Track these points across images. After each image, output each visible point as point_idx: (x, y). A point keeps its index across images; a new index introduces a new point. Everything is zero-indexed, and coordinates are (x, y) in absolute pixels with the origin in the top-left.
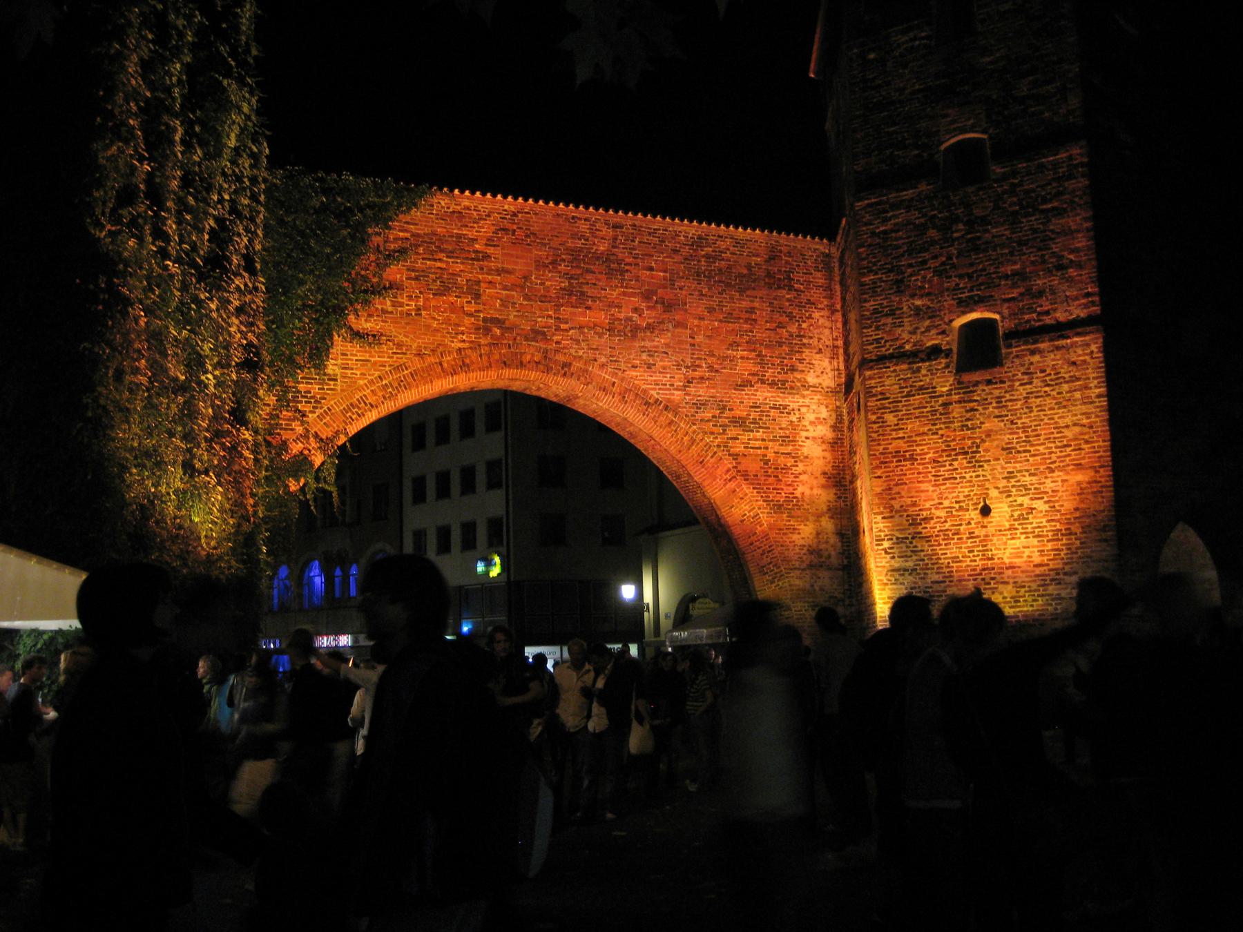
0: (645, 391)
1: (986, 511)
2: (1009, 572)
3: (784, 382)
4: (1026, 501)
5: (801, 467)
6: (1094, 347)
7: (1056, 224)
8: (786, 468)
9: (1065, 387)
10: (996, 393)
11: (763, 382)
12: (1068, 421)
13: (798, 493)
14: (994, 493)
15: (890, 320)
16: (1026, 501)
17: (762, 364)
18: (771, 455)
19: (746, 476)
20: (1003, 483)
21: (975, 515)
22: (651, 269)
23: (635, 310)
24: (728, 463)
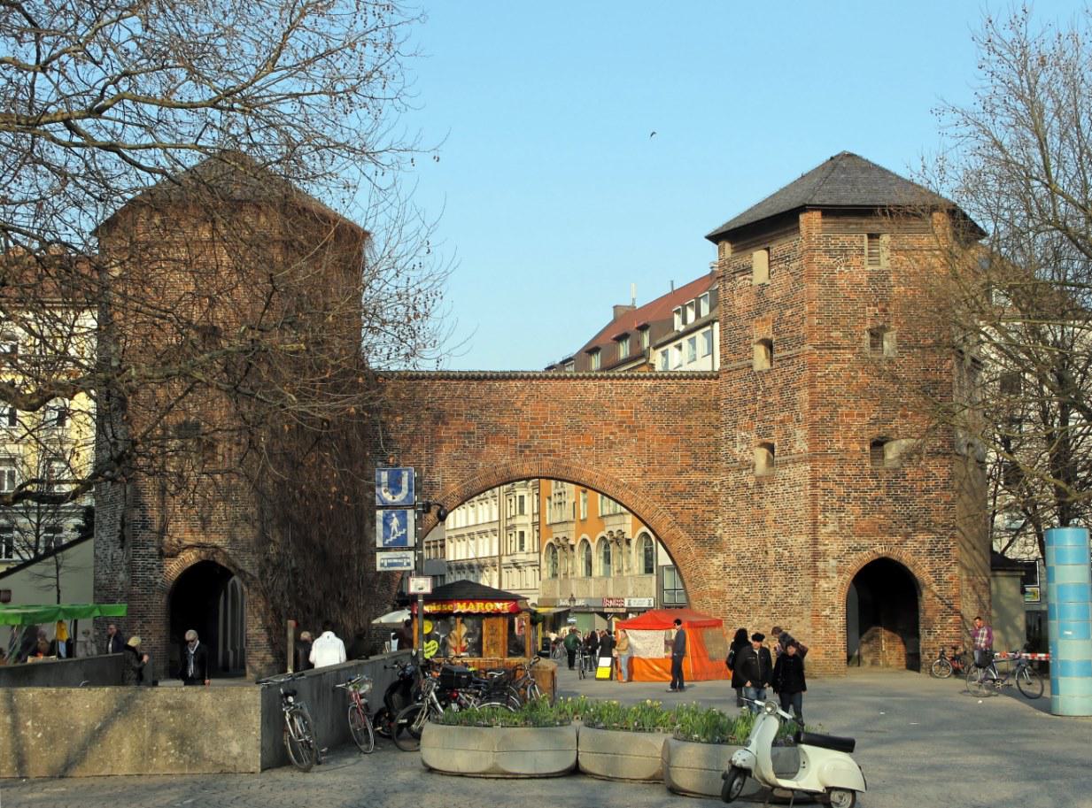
0: (617, 480)
1: (766, 552)
2: (773, 589)
3: (710, 468)
8: (710, 520)
9: (797, 489)
10: (771, 489)
11: (696, 469)
13: (717, 534)
14: (769, 545)
15: (731, 443)
16: (780, 550)
18: (699, 512)
19: (681, 525)
20: (772, 540)
22: (623, 408)
23: (612, 433)
24: (670, 518)
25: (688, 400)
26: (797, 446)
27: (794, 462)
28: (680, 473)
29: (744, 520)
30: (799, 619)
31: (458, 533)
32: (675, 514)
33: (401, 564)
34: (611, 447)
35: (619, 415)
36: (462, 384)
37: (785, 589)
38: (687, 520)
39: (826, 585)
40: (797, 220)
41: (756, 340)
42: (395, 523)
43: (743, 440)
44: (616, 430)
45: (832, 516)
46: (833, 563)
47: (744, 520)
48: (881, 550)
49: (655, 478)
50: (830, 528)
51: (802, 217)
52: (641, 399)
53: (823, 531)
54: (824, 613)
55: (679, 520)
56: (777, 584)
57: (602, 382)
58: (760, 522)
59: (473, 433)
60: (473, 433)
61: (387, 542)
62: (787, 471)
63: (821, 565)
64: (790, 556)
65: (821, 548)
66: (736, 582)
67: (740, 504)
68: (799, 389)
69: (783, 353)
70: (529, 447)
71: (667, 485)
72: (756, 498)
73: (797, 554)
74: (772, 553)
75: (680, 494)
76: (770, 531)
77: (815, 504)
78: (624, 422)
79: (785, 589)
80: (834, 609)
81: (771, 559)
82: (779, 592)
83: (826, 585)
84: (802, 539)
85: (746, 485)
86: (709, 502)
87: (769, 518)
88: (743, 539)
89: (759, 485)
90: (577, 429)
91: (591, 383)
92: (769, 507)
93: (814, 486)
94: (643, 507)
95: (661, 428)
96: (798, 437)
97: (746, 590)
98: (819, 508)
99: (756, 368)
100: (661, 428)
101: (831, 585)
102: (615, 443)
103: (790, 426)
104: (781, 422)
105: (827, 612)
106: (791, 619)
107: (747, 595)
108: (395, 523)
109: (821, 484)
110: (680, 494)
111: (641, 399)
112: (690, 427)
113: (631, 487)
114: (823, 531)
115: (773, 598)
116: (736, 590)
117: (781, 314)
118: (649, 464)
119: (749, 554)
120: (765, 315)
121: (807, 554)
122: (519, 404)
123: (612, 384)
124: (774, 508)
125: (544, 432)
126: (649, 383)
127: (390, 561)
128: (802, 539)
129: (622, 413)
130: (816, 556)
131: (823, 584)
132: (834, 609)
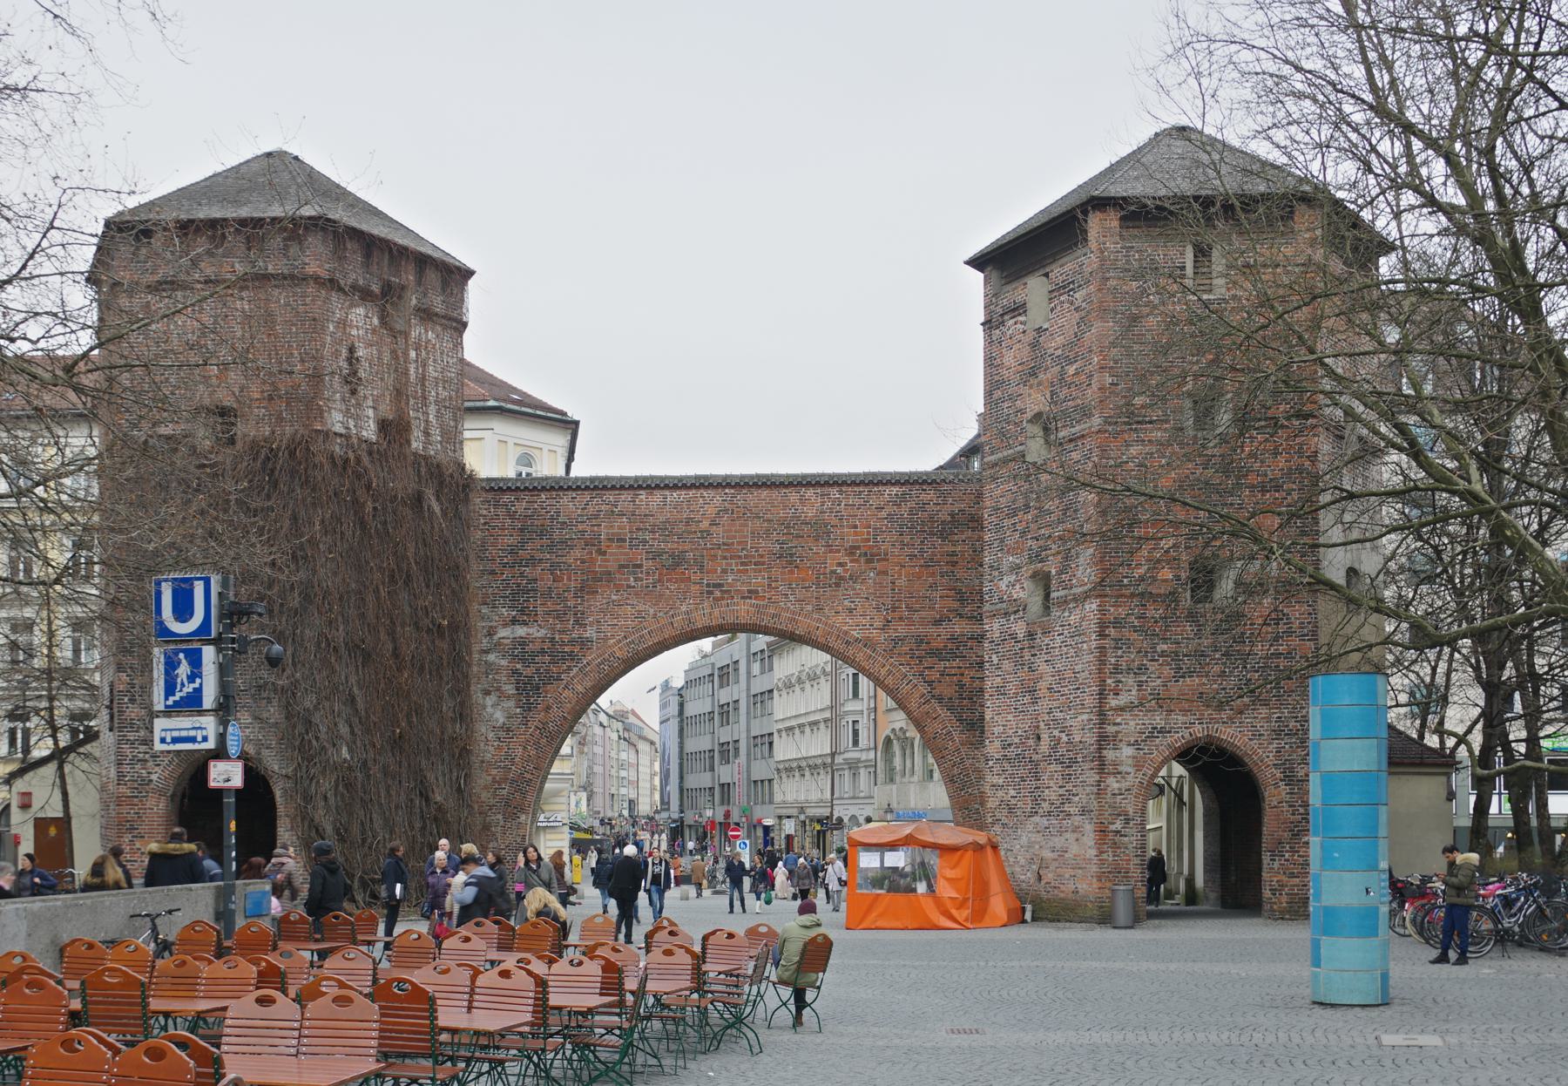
0: (846, 633)
1: (1039, 738)
6: (1094, 606)
11: (961, 616)
16: (1056, 733)
17: (961, 600)
19: (940, 699)
21: (1031, 742)
23: (840, 565)
25: (952, 515)
28: (937, 622)
29: (1011, 688)
31: (812, 718)
32: (930, 683)
33: (193, 740)
34: (837, 585)
35: (851, 540)
36: (626, 496)
37: (1062, 791)
38: (948, 691)
39: (1116, 785)
41: (1029, 415)
42: (183, 670)
44: (847, 559)
45: (1130, 680)
46: (1128, 751)
47: (1011, 688)
48: (1199, 731)
49: (901, 630)
50: (1123, 700)
52: (884, 514)
53: (1114, 703)
54: (1113, 827)
55: (936, 692)
57: (826, 490)
58: (1032, 691)
59: (640, 566)
60: (640, 566)
61: (170, 702)
63: (1110, 755)
65: (1111, 729)
70: (720, 585)
71: (920, 640)
74: (1045, 736)
75: (937, 654)
76: (1044, 705)
77: (1102, 662)
78: (858, 548)
79: (1062, 791)
80: (1127, 821)
81: (1044, 747)
83: (1116, 785)
85: (1013, 636)
87: (1043, 685)
88: (1010, 717)
89: (1031, 635)
90: (787, 558)
91: (810, 492)
92: (1043, 668)
93: (1102, 635)
94: (883, 672)
95: (912, 557)
97: (1013, 793)
98: (1108, 668)
100: (912, 557)
101: (1124, 785)
102: (842, 578)
105: (1118, 825)
107: (1013, 801)
108: (183, 670)
109: (1112, 631)
110: (937, 654)
111: (884, 514)
112: (954, 554)
113: (867, 643)
116: (1000, 793)
117: (1062, 373)
118: (894, 609)
119: (1017, 740)
121: (1090, 738)
122: (705, 524)
123: (841, 492)
124: (1049, 669)
125: (743, 564)
126: (895, 490)
127: (176, 734)
129: (856, 534)
130: (1103, 740)
131: (1113, 783)
132: (1127, 821)
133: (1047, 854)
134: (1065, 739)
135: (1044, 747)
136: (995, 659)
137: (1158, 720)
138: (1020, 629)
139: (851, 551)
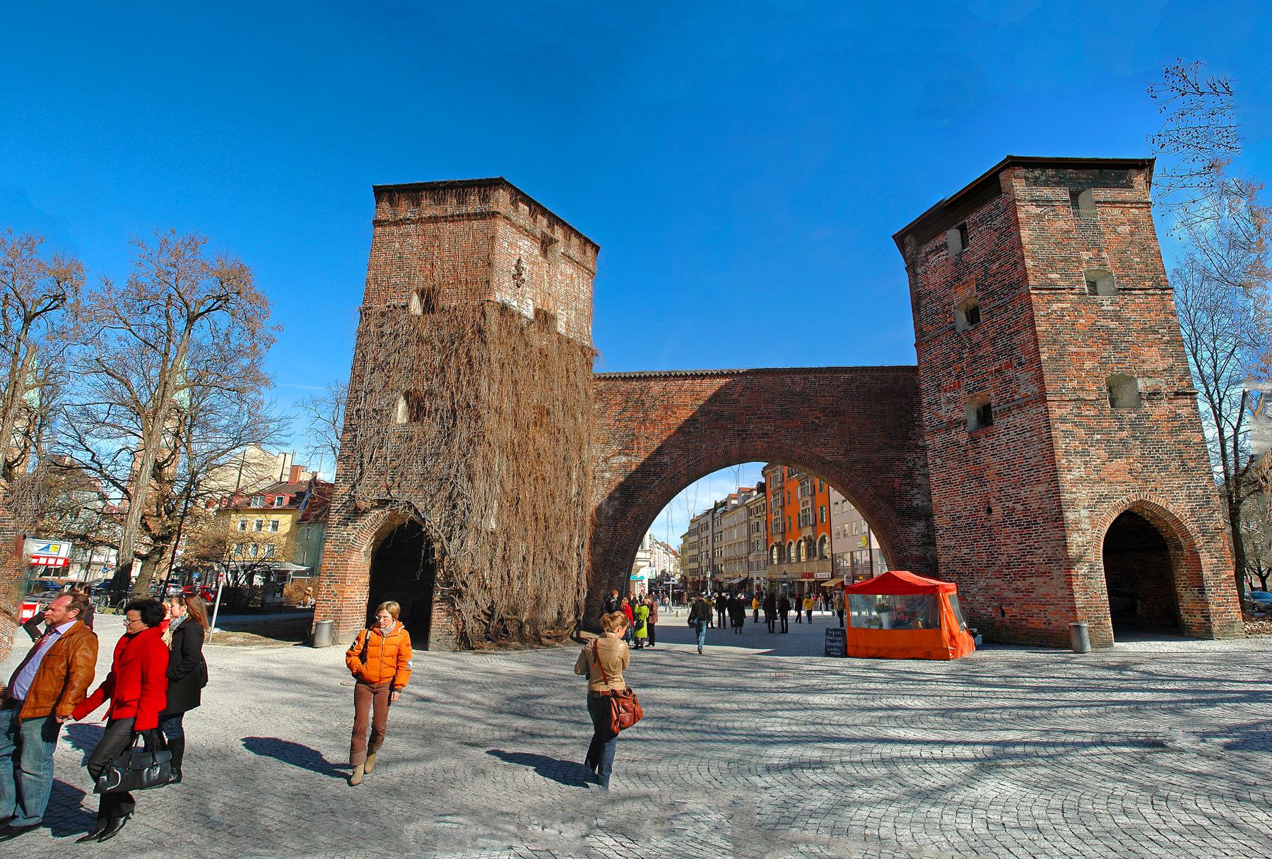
1: (990, 511)
4: (1010, 504)
5: (915, 491)
7: (1016, 339)
9: (1028, 434)
12: (1031, 454)
16: (1010, 504)
18: (896, 485)
21: (983, 514)
26: (1022, 391)
27: (1019, 407)
28: (877, 451)
30: (1048, 580)
32: (875, 487)
37: (1020, 547)
40: (998, 179)
43: (949, 401)
46: (1084, 513)
50: (1076, 474)
51: (1002, 176)
53: (1069, 477)
56: (1008, 541)
62: (1011, 419)
64: (1026, 510)
66: (953, 543)
67: (950, 463)
68: (1018, 332)
69: (993, 305)
72: (971, 454)
73: (1035, 506)
79: (1020, 547)
82: (1011, 551)
84: (1041, 488)
85: (956, 444)
86: (906, 476)
89: (974, 440)
95: (859, 413)
96: (1022, 381)
99: (958, 330)
103: (1010, 373)
104: (996, 371)
106: (1033, 579)
114: (1069, 477)
115: (1004, 558)
120: (966, 278)
128: (1041, 488)
133: (1009, 594)
134: (1019, 507)
135: (997, 512)
136: (938, 461)
137: (1104, 489)
138: (963, 438)
139: (823, 410)
